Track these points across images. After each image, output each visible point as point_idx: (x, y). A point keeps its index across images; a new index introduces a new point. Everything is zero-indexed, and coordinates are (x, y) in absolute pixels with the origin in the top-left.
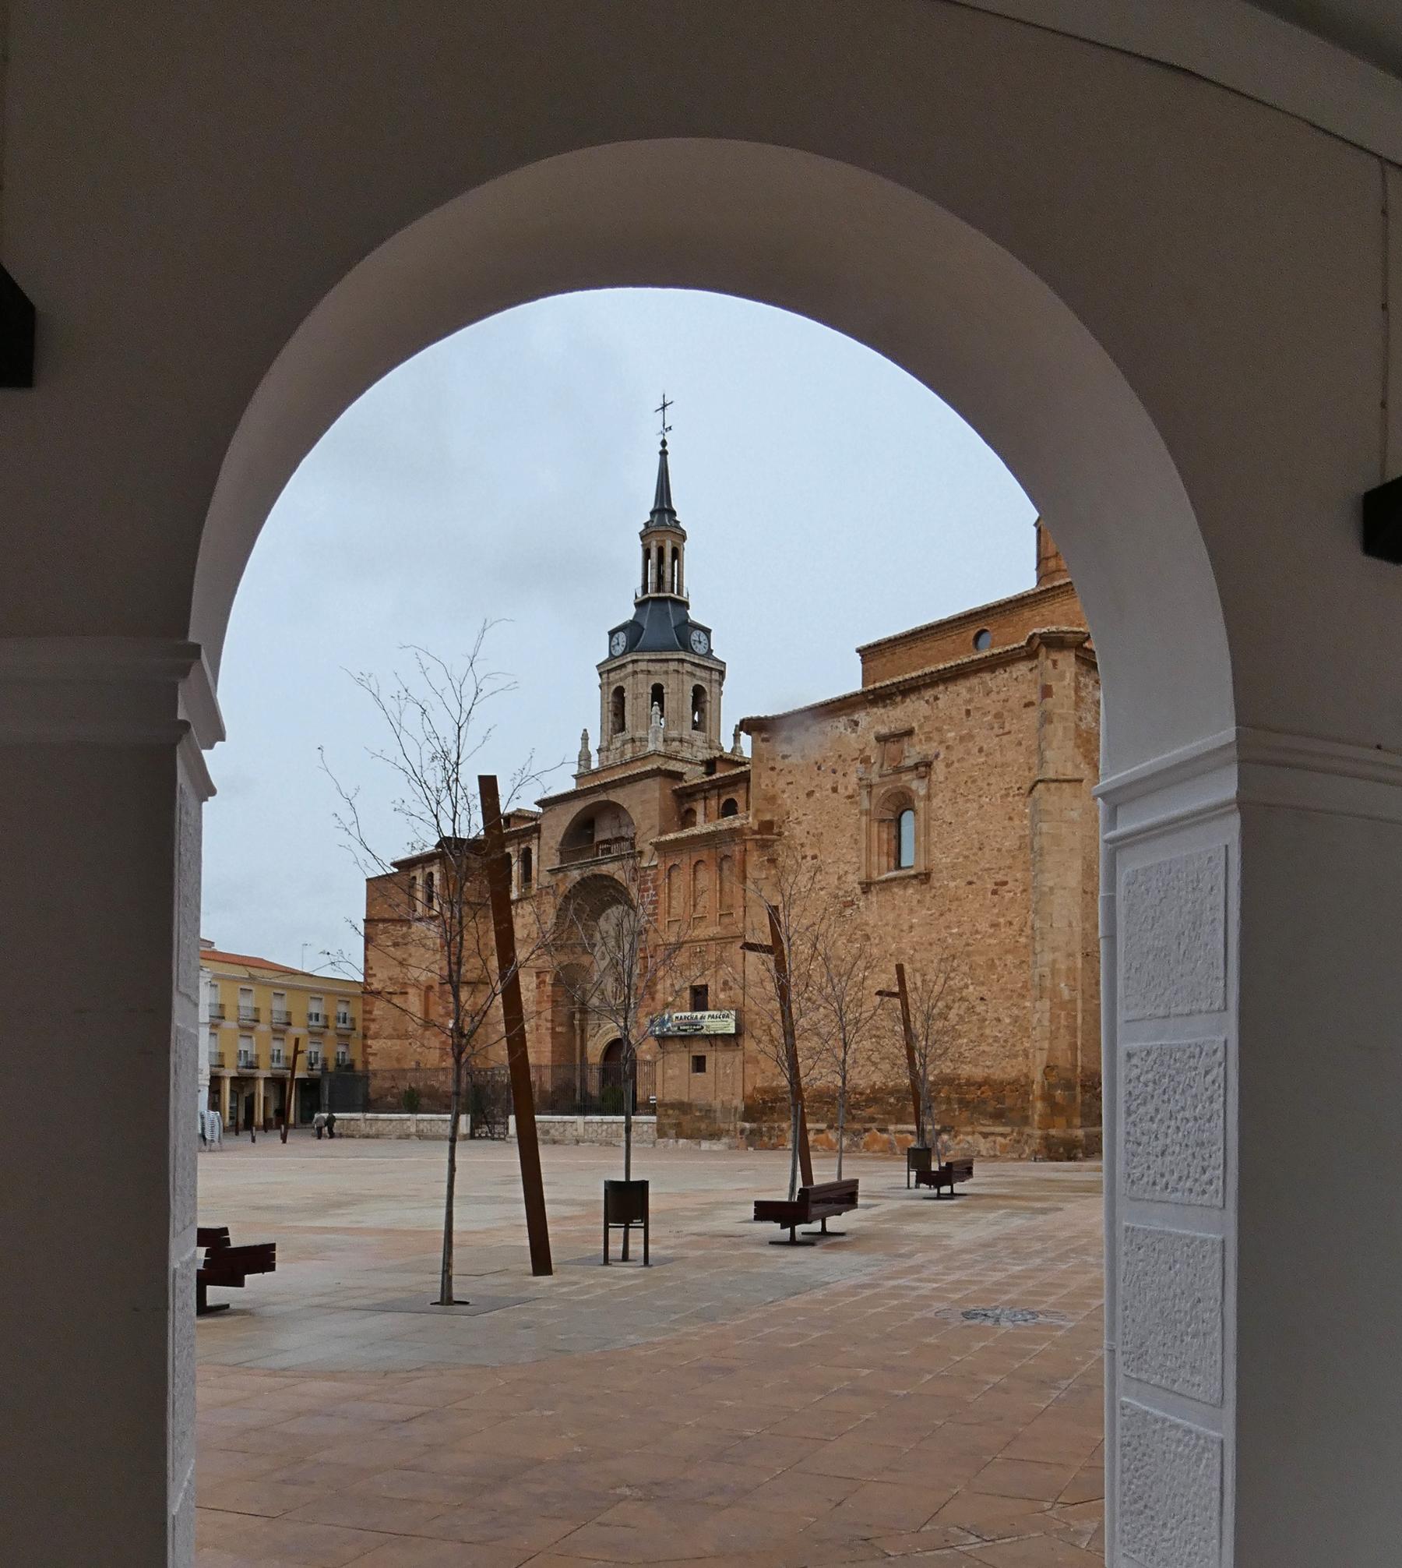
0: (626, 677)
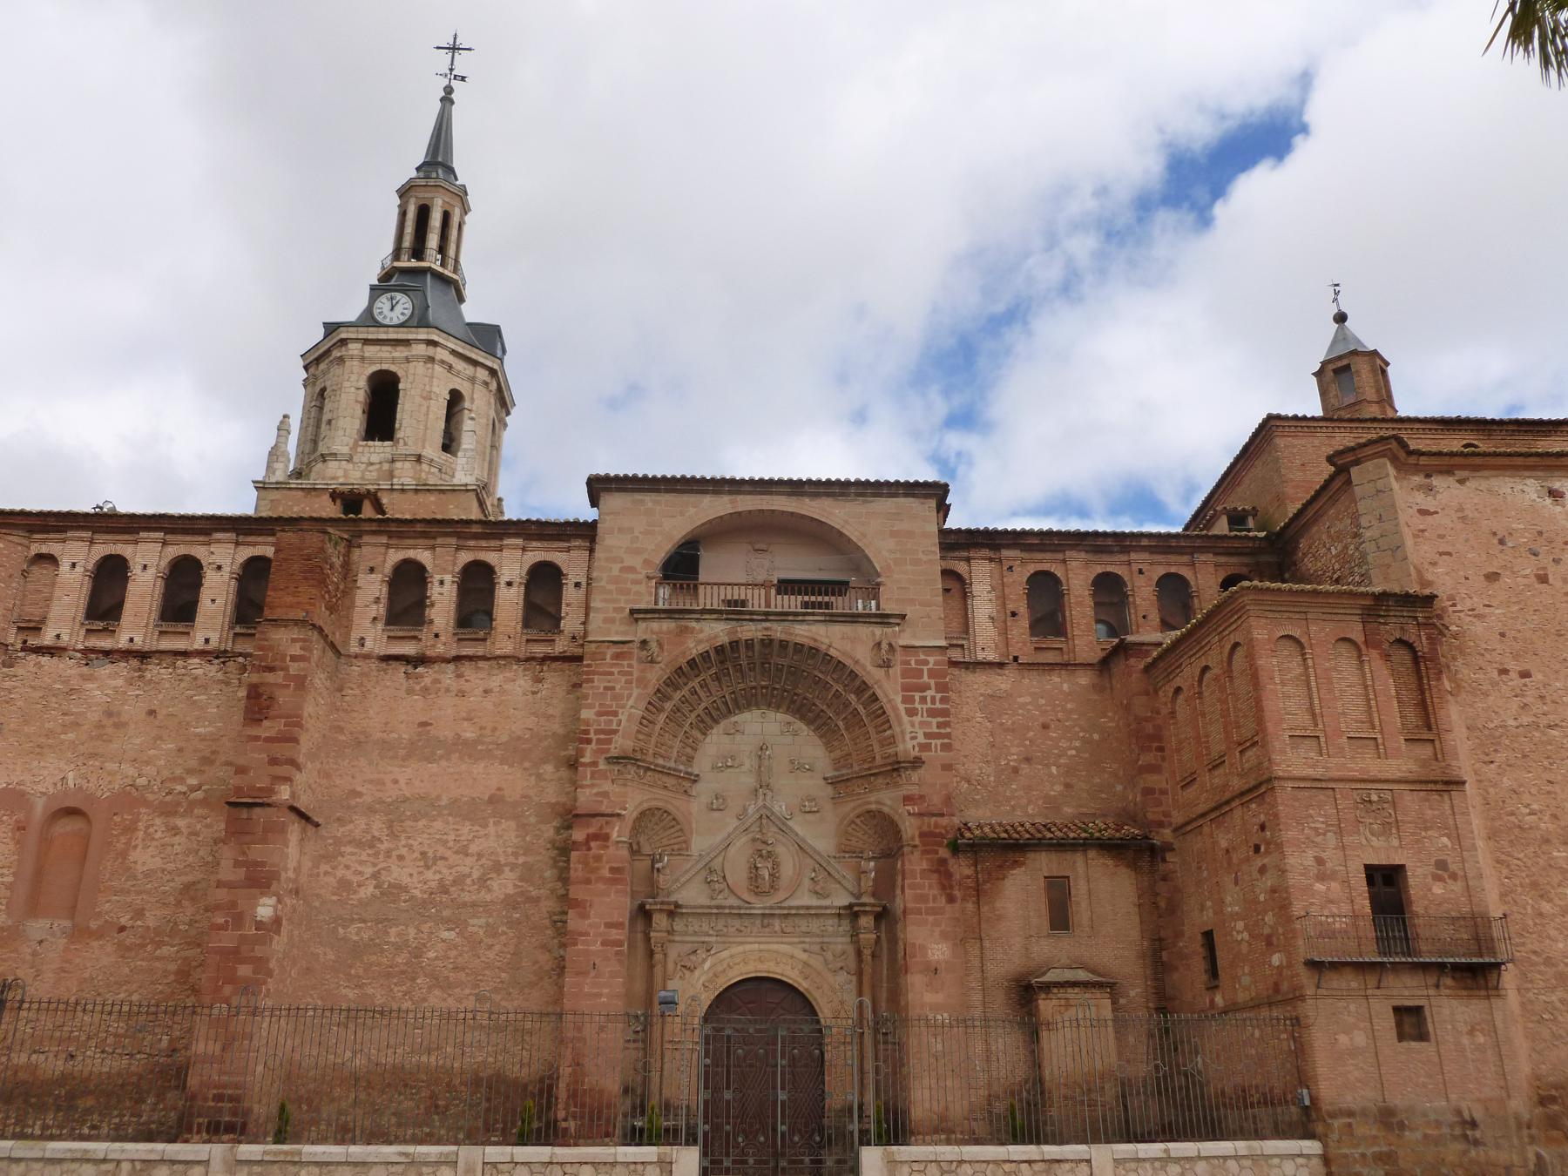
0: (407, 360)
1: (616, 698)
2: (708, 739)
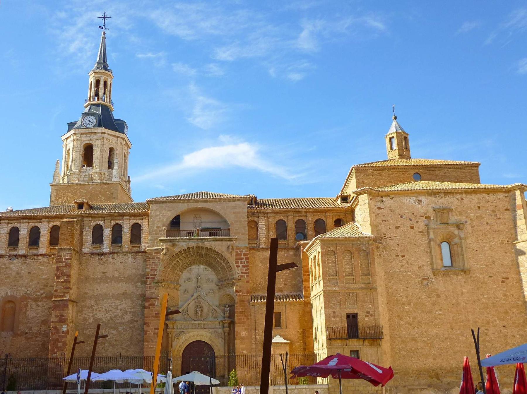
1: (156, 265)
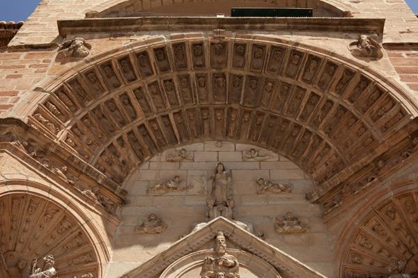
2: (145, 166)
